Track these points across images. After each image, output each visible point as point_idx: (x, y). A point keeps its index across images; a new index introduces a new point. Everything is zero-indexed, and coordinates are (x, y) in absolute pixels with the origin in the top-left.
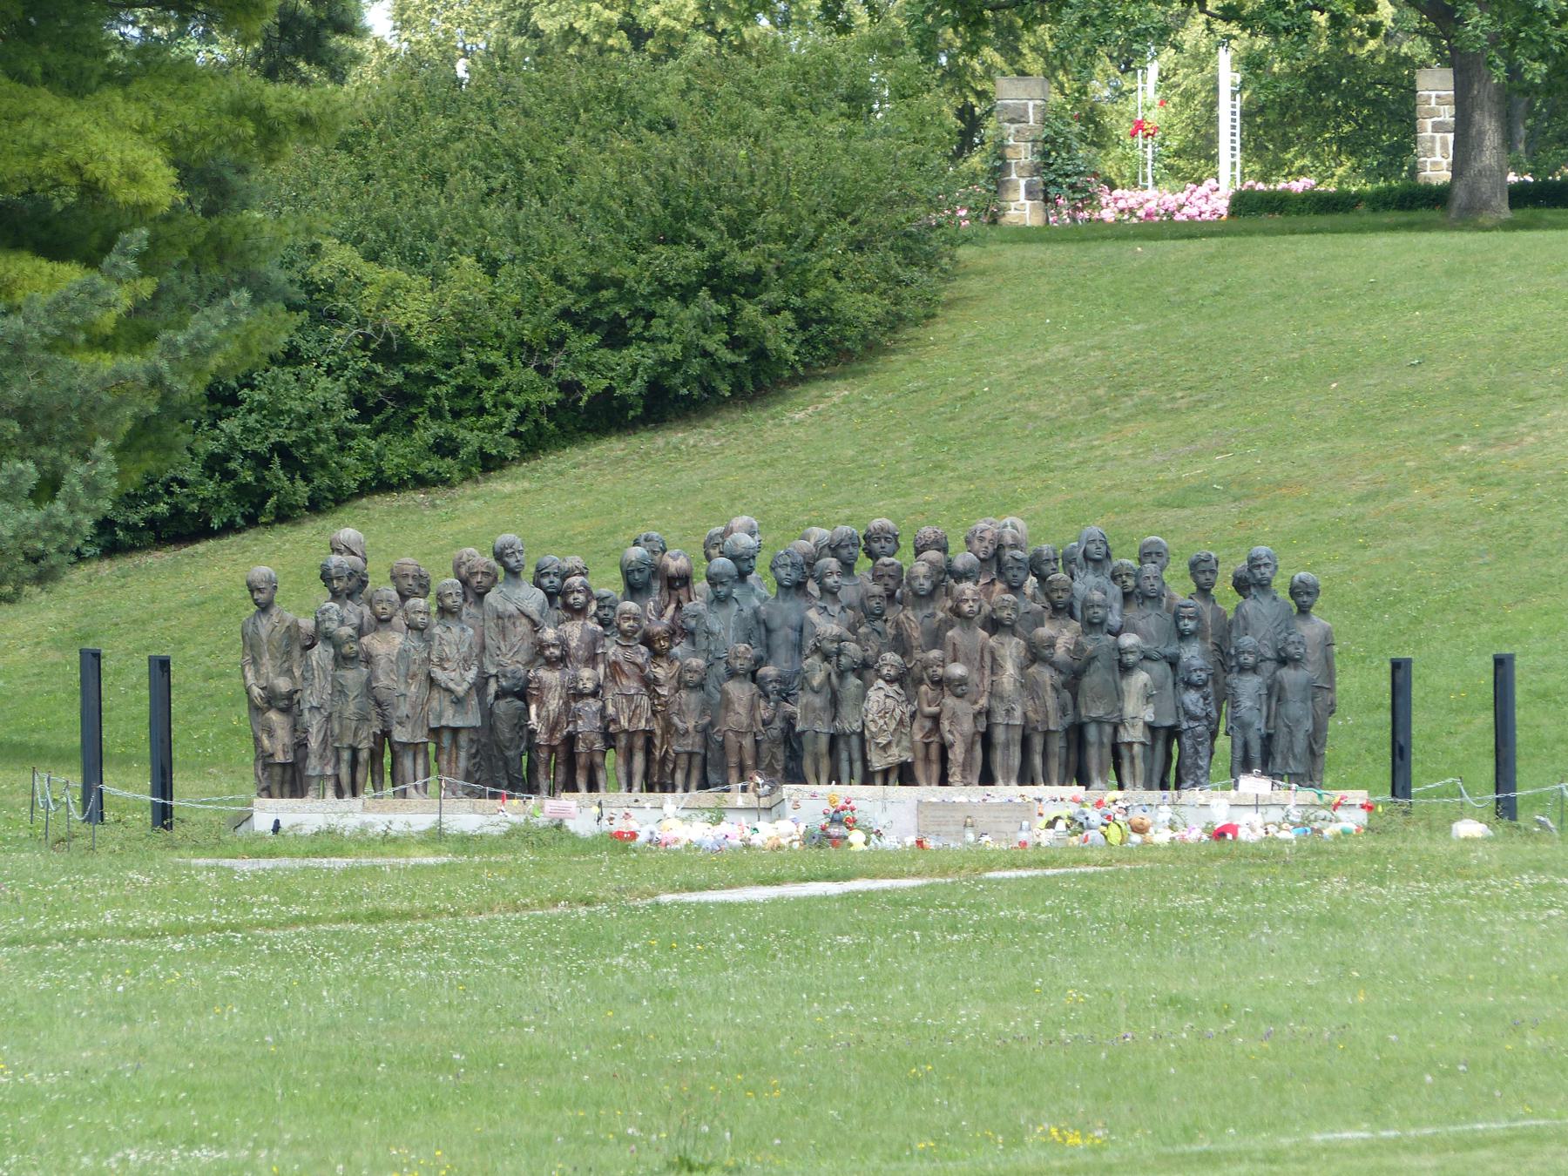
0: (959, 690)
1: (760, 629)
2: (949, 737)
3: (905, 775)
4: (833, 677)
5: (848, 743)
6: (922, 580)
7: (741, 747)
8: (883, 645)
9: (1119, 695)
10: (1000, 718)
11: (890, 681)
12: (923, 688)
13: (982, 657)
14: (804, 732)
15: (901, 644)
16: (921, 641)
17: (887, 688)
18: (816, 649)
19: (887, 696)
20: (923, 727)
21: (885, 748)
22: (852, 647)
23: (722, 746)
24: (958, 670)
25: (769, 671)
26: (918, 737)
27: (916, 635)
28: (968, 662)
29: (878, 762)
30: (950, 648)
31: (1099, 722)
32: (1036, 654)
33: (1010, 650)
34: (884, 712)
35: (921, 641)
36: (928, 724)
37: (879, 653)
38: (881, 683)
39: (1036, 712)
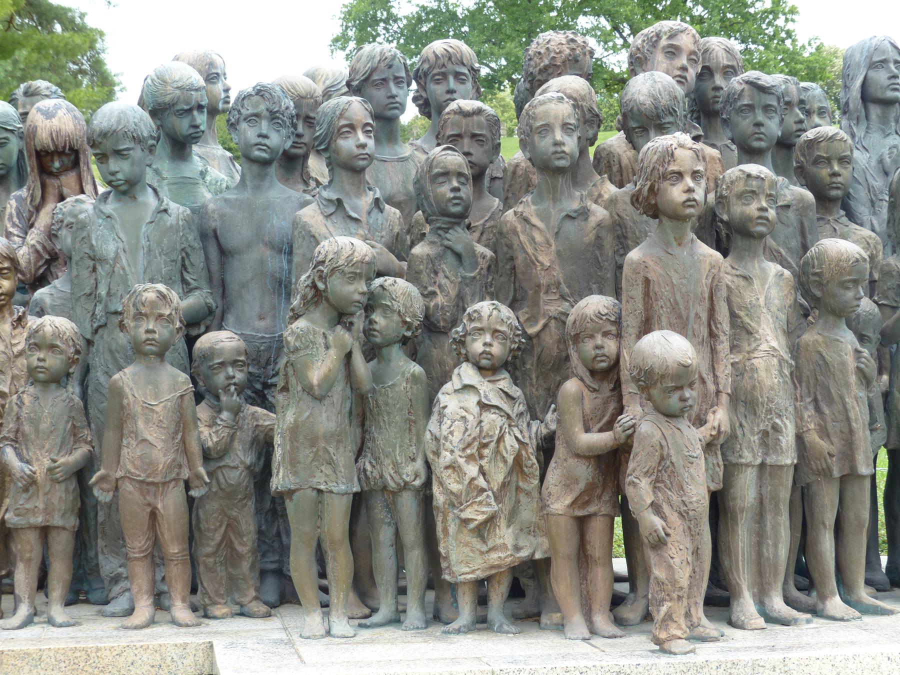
0: (674, 401)
1: (209, 253)
2: (651, 521)
3: (525, 597)
4: (358, 359)
5: (392, 509)
6: (559, 135)
7: (153, 515)
8: (465, 282)
10: (750, 455)
11: (488, 368)
12: (571, 386)
13: (712, 312)
14: (291, 492)
15: (507, 276)
16: (558, 273)
17: (489, 390)
18: (317, 296)
19: (484, 407)
20: (568, 482)
21: (483, 530)
22: (401, 288)
23: (113, 506)
24: (668, 346)
25: (221, 340)
26: (560, 504)
27: (545, 259)
28: (681, 326)
29: (464, 561)
30: (638, 292)
32: (816, 296)
33: (768, 285)
34: (479, 446)
35: (558, 273)
36: (584, 472)
37: (460, 303)
38: (467, 373)
39: (824, 432)
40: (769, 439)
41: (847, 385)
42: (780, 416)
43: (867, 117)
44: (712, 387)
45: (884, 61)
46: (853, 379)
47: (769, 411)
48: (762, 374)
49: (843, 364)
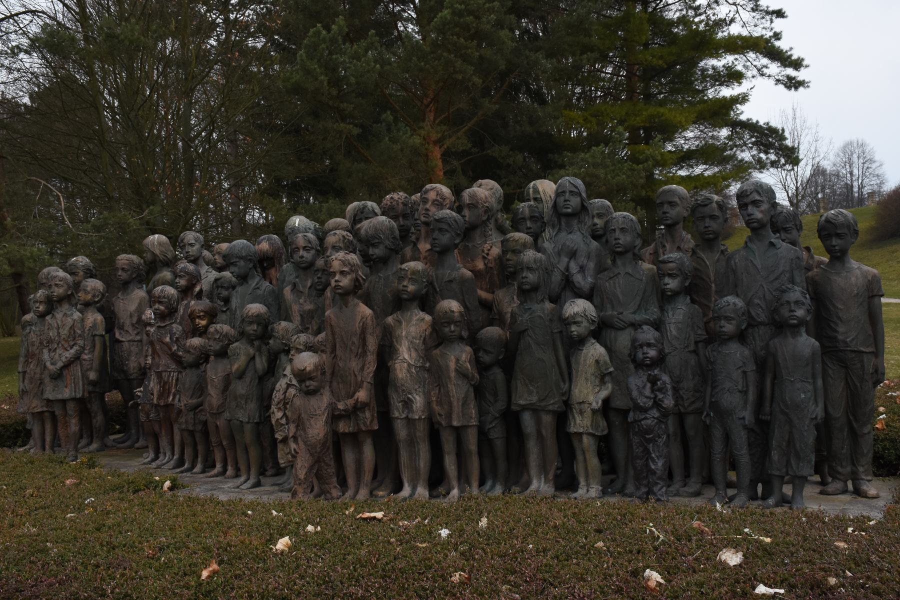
7: (217, 426)
9: (568, 374)
10: (397, 412)
31: (535, 410)
40: (408, 404)
41: (450, 378)
42: (410, 394)
43: (560, 224)
44: (359, 379)
45: (564, 192)
46: (453, 374)
47: (403, 390)
48: (398, 371)
49: (448, 366)
